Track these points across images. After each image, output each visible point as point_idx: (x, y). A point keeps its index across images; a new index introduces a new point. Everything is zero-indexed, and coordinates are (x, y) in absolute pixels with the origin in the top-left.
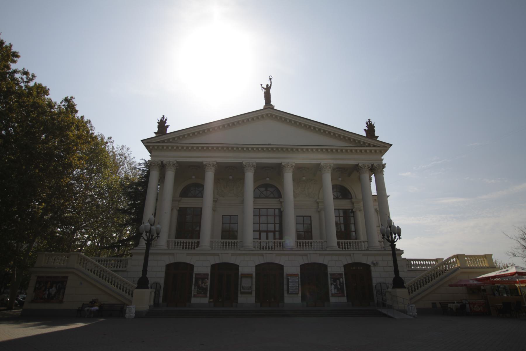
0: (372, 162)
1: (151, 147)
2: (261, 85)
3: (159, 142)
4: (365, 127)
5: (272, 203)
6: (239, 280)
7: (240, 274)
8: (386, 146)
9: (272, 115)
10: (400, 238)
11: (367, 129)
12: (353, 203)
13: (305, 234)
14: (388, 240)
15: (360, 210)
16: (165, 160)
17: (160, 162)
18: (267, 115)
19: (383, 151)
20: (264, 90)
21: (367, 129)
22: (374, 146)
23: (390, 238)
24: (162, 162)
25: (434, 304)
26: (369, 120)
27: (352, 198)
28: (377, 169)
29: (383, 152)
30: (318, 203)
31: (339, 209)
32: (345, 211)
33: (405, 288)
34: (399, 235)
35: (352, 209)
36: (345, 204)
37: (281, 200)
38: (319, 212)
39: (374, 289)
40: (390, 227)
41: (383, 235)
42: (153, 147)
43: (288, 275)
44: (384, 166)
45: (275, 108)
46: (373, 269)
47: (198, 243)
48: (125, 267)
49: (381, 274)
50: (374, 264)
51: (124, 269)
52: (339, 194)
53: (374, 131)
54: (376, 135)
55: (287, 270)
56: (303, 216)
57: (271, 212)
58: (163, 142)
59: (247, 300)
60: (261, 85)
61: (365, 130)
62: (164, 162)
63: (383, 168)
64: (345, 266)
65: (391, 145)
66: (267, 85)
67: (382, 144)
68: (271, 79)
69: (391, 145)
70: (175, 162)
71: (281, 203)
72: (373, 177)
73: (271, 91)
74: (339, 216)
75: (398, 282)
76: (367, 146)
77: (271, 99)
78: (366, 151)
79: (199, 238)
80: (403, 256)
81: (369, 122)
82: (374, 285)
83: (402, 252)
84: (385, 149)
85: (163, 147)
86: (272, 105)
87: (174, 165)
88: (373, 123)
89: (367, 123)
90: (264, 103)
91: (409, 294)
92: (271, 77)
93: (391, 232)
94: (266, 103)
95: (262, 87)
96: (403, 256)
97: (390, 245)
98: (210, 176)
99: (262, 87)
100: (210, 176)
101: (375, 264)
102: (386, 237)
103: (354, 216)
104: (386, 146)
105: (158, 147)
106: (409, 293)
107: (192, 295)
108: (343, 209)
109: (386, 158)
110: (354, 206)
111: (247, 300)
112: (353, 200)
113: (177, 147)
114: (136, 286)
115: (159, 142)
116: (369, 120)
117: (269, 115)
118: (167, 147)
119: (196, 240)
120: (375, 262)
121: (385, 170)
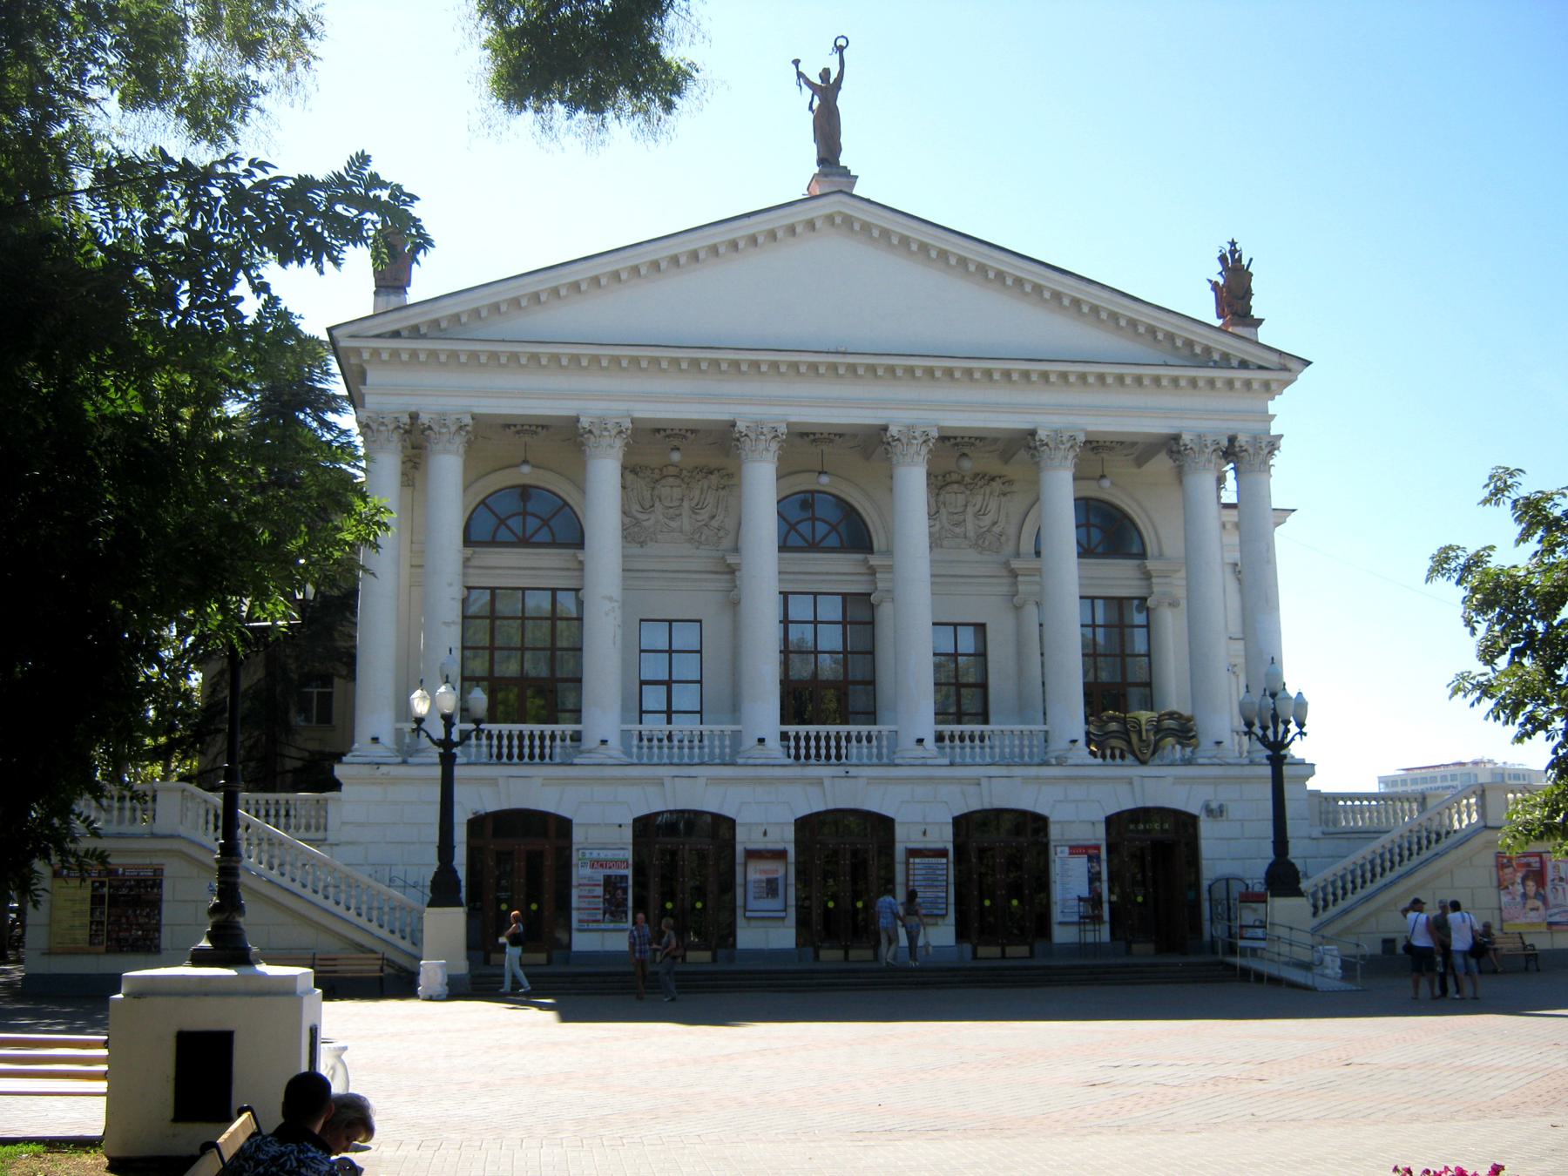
0: (1232, 426)
1: (366, 356)
2: (796, 62)
3: (396, 334)
4: (1214, 271)
5: (837, 571)
6: (739, 869)
7: (739, 848)
8: (1288, 366)
9: (848, 221)
10: (1302, 734)
11: (1221, 281)
12: (1147, 576)
13: (964, 694)
14: (1263, 740)
15: (1174, 604)
16: (428, 408)
17: (406, 419)
18: (830, 219)
19: (1274, 386)
20: (808, 92)
21: (1221, 281)
22: (1244, 365)
23: (1270, 733)
24: (414, 417)
25: (1388, 944)
26: (1233, 244)
27: (1143, 555)
28: (1247, 453)
29: (1270, 390)
30: (1014, 574)
31: (1093, 598)
32: (1118, 604)
33: (1298, 893)
34: (1301, 725)
35: (1143, 600)
36: (1118, 577)
37: (874, 560)
38: (1018, 609)
39: (1205, 895)
40: (1273, 695)
41: (1249, 724)
42: (376, 352)
43: (913, 853)
44: (1273, 445)
45: (858, 190)
46: (1206, 829)
47: (577, 737)
48: (317, 829)
49: (1230, 850)
50: (1210, 812)
51: (320, 835)
52: (1096, 535)
53: (1248, 294)
54: (1256, 313)
55: (905, 837)
56: (955, 625)
57: (831, 609)
58: (415, 332)
59: (767, 932)
60: (796, 62)
61: (1215, 286)
62: (424, 419)
63: (1271, 453)
64: (1110, 821)
65: (1309, 363)
66: (825, 74)
67: (1275, 358)
68: (840, 49)
69: (1309, 363)
70: (468, 420)
71: (872, 571)
72: (1231, 475)
73: (843, 101)
74: (1094, 626)
75: (1283, 878)
76: (1216, 365)
77: (843, 140)
78: (1211, 383)
79: (578, 721)
80: (1311, 784)
81: (1233, 252)
82: (1205, 883)
83: (1310, 769)
84: (1284, 375)
85: (414, 354)
86: (845, 172)
87: (461, 428)
88: (1245, 262)
89: (1222, 259)
90: (807, 161)
91: (1315, 914)
92: (842, 42)
93: (1272, 721)
94: (821, 161)
95: (800, 75)
96: (1311, 784)
97: (1268, 757)
98: (605, 476)
99: (800, 75)
100: (605, 476)
101: (1216, 812)
102: (1257, 729)
103: (1148, 626)
104: (1288, 366)
105: (395, 353)
106: (1315, 906)
107: (575, 924)
108: (1107, 599)
109: (1288, 412)
110: (1150, 586)
111: (767, 932)
112: (1151, 564)
113: (474, 355)
114: (427, 899)
115: (396, 334)
116: (1233, 244)
117: (838, 220)
118: (433, 354)
119: (569, 728)
120: (1214, 805)
121: (1277, 461)
